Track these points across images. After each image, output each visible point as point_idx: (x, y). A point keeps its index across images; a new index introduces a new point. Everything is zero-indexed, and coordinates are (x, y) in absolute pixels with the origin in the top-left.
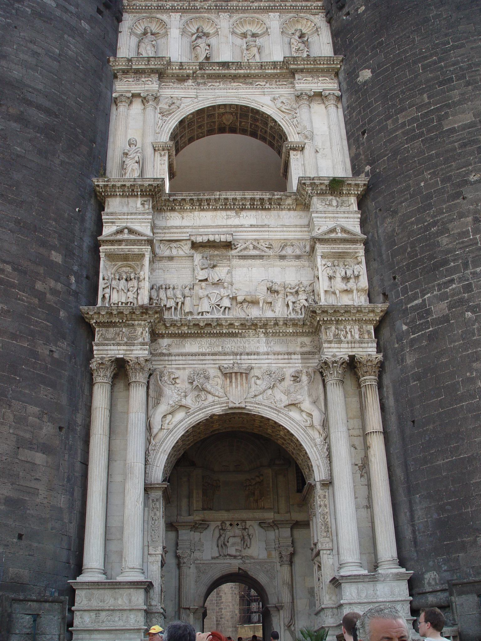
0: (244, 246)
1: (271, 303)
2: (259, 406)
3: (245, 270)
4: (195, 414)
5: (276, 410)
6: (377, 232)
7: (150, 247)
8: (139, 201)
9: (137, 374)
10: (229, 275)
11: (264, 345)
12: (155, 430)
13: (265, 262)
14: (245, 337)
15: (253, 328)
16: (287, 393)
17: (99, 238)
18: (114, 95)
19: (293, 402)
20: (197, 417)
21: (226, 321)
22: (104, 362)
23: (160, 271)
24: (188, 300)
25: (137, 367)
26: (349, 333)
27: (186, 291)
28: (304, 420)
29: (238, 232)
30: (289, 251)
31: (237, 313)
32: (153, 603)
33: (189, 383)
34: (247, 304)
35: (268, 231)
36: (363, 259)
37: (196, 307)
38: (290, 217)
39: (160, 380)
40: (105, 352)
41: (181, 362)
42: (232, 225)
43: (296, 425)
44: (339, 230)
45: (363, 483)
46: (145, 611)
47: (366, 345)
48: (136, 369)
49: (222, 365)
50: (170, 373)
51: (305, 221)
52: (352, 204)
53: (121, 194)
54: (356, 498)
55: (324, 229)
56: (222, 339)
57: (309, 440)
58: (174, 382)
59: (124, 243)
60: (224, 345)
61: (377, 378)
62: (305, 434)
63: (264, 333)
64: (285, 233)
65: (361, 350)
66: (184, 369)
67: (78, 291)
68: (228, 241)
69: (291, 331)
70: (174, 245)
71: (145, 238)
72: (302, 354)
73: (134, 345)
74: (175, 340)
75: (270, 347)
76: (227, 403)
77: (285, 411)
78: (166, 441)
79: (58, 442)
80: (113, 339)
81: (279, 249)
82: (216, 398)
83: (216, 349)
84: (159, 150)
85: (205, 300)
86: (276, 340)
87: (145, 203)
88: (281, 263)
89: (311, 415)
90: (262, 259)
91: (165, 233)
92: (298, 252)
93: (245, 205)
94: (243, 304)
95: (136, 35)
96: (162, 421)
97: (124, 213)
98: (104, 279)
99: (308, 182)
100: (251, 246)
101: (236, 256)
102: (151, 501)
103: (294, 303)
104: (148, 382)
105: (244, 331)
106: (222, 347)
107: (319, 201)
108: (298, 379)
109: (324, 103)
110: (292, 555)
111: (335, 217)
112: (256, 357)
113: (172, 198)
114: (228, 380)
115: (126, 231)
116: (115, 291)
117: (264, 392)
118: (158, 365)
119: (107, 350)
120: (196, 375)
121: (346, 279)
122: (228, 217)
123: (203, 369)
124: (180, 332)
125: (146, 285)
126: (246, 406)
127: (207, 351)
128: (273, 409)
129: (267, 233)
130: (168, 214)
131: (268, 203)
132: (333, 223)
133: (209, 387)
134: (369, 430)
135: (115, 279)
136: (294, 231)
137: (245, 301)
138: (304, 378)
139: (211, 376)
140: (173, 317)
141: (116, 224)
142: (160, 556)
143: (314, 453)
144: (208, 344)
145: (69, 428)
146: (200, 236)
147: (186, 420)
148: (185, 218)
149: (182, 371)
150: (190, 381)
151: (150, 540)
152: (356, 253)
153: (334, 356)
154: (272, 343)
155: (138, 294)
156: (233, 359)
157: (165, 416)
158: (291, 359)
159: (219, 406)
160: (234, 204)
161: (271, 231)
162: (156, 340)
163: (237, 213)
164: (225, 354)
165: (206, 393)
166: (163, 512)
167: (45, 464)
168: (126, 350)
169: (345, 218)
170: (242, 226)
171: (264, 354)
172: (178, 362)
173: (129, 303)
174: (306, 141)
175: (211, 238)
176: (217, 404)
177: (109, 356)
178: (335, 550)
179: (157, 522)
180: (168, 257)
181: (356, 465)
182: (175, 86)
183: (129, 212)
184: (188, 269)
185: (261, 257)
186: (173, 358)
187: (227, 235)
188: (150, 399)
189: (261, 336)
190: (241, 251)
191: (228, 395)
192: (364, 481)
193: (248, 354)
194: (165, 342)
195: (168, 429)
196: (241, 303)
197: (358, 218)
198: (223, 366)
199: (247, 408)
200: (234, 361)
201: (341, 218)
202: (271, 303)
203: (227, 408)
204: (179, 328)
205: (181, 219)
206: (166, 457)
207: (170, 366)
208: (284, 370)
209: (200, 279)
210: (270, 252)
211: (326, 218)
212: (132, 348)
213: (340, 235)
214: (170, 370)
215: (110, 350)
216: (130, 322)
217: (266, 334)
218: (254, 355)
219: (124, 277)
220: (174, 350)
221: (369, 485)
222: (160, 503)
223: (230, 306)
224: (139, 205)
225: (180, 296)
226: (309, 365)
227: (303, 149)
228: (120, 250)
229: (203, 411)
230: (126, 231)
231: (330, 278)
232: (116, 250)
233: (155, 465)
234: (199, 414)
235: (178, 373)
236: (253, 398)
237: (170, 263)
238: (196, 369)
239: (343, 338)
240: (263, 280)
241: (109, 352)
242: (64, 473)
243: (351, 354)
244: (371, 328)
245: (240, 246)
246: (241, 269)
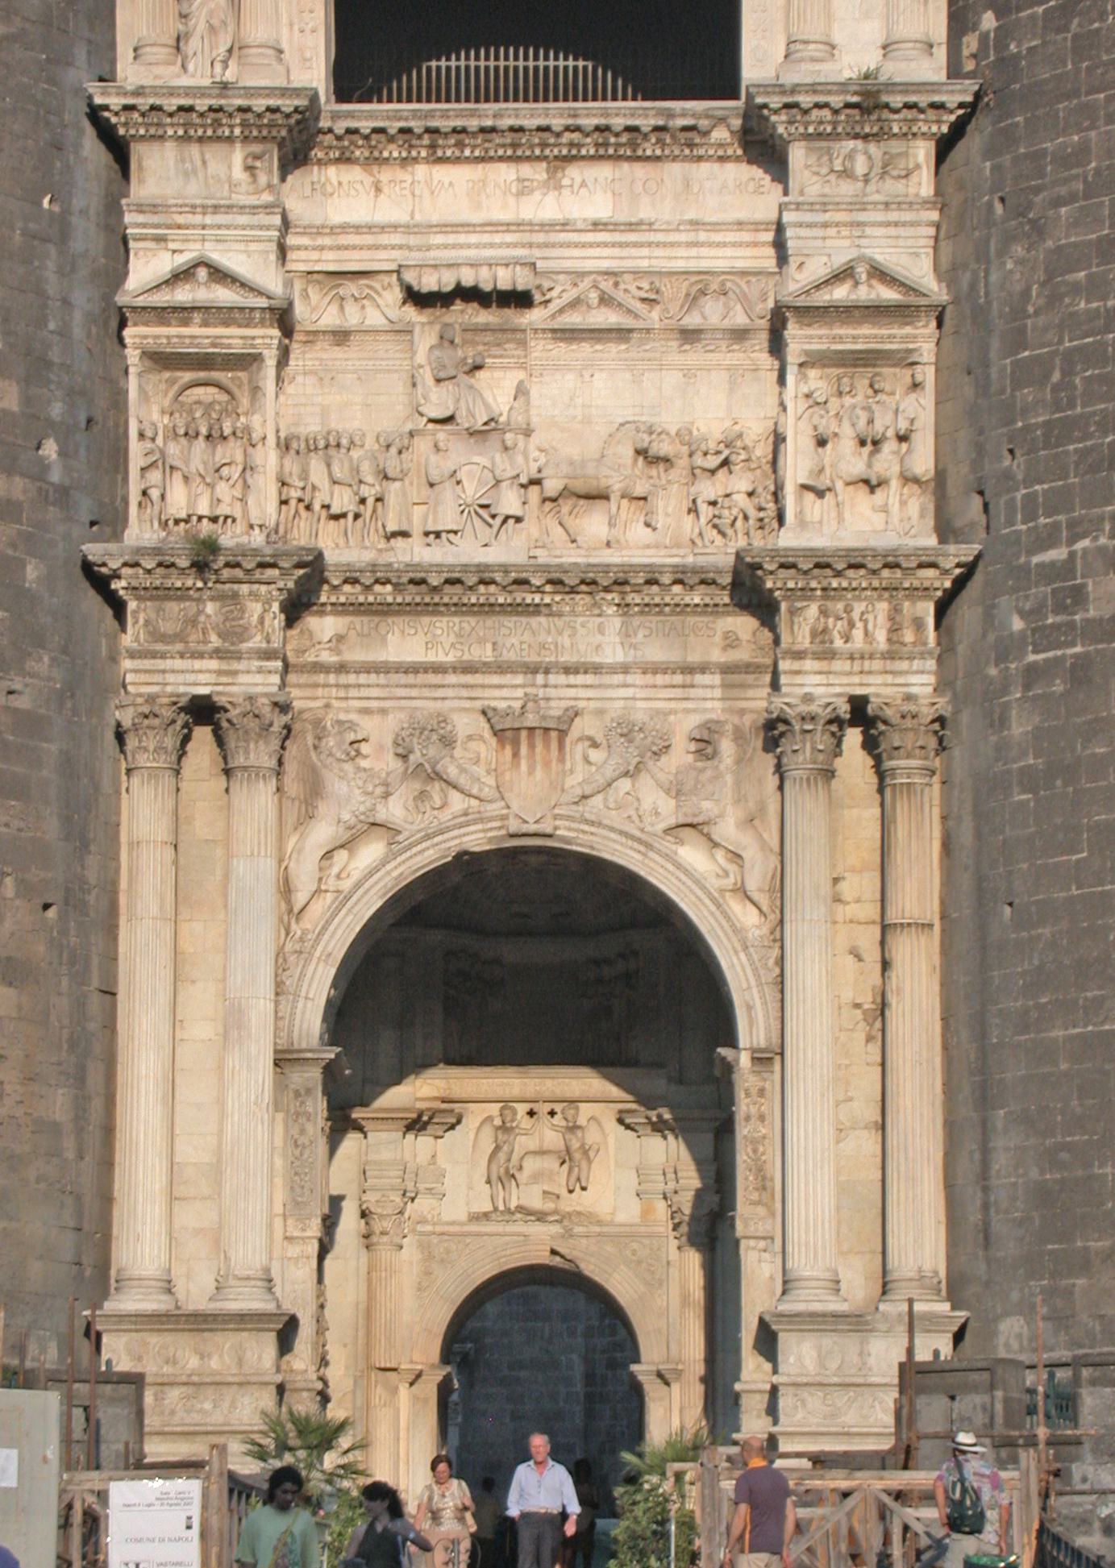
0: (572, 294)
2: (593, 829)
3: (570, 380)
4: (414, 850)
5: (639, 841)
6: (986, 277)
7: (276, 332)
8: (238, 155)
9: (252, 746)
10: (521, 400)
11: (618, 639)
12: (300, 899)
14: (560, 615)
15: (584, 588)
16: (677, 791)
19: (689, 820)
20: (419, 858)
22: (156, 709)
23: (311, 380)
25: (253, 724)
26: (859, 625)
27: (388, 463)
28: (720, 873)
29: (553, 245)
30: (711, 313)
33: (397, 755)
34: (571, 502)
35: (650, 244)
36: (930, 371)
38: (724, 186)
39: (315, 747)
40: (158, 678)
41: (374, 692)
42: (536, 221)
43: (694, 887)
44: (861, 271)
47: (904, 665)
49: (493, 704)
50: (343, 726)
52: (918, 167)
53: (181, 132)
55: (817, 268)
56: (491, 621)
57: (729, 931)
58: (353, 753)
59: (197, 317)
60: (500, 640)
62: (718, 913)
63: (618, 605)
64: (704, 251)
65: (889, 679)
66: (383, 712)
67: (67, 482)
68: (520, 288)
69: (697, 600)
70: (350, 288)
71: (263, 302)
72: (727, 669)
73: (240, 658)
75: (634, 646)
76: (504, 818)
77: (667, 845)
78: (332, 928)
79: (42, 949)
80: (180, 637)
81: (682, 306)
82: (474, 803)
85: (448, 492)
86: (653, 626)
87: (258, 164)
88: (682, 357)
89: (739, 856)
90: (627, 340)
91: (322, 248)
92: (740, 319)
93: (579, 146)
94: (560, 501)
96: (321, 869)
97: (194, 206)
98: (142, 436)
99: (775, 102)
100: (594, 296)
101: (544, 330)
102: (291, 1095)
103: (713, 503)
105: (558, 598)
106: (494, 644)
107: (812, 160)
108: (709, 750)
111: (859, 224)
112: (589, 679)
114: (508, 751)
115: (202, 273)
116: (178, 476)
117: (609, 785)
119: (164, 672)
120: (417, 732)
122: (524, 189)
123: (439, 715)
124: (371, 599)
126: (556, 828)
127: (450, 658)
129: (645, 251)
130: (332, 171)
131: (653, 140)
132: (847, 243)
133: (452, 772)
136: (734, 245)
137: (567, 493)
141: (172, 246)
143: (738, 968)
144: (452, 636)
145: (67, 903)
146: (431, 270)
147: (389, 867)
148: (386, 189)
149: (377, 719)
150: (400, 751)
152: (910, 351)
153: (808, 698)
154: (640, 635)
155: (246, 486)
156: (523, 686)
157: (328, 855)
158: (693, 686)
159: (479, 827)
160: (544, 145)
161: (658, 245)
162: (298, 618)
163: (552, 172)
164: (502, 668)
165: (444, 785)
167: (14, 1015)
168: (220, 673)
169: (888, 224)
170: (565, 226)
171: (613, 669)
172: (364, 692)
173: (221, 519)
175: (468, 278)
176: (475, 822)
177: (169, 689)
179: (307, 1153)
180: (334, 333)
181: (857, 1006)
183: (210, 202)
184: (396, 376)
185: (621, 334)
186: (352, 678)
187: (518, 268)
189: (610, 612)
190: (561, 311)
191: (506, 795)
193: (568, 670)
195: (338, 891)
196: (554, 500)
197: (930, 224)
198: (495, 710)
199: (558, 832)
200: (529, 690)
201: (874, 224)
202: (645, 499)
203: (503, 832)
204: (368, 588)
205: (373, 193)
206: (333, 971)
207: (343, 704)
208: (672, 718)
209: (434, 415)
211: (825, 225)
214: (342, 717)
215: (173, 671)
216: (228, 586)
217: (624, 607)
218: (586, 672)
219: (204, 431)
220: (356, 655)
223: (519, 513)
224: (238, 173)
225: (370, 479)
228: (187, 341)
229: (436, 840)
230: (202, 273)
232: (175, 340)
233: (303, 994)
234: (424, 850)
235: (368, 726)
236: (576, 803)
237: (338, 352)
238: (418, 713)
239: (838, 643)
240: (622, 425)
241: (170, 678)
242: (62, 1028)
243: (859, 691)
244: (927, 610)
245: (562, 293)
246: (558, 376)
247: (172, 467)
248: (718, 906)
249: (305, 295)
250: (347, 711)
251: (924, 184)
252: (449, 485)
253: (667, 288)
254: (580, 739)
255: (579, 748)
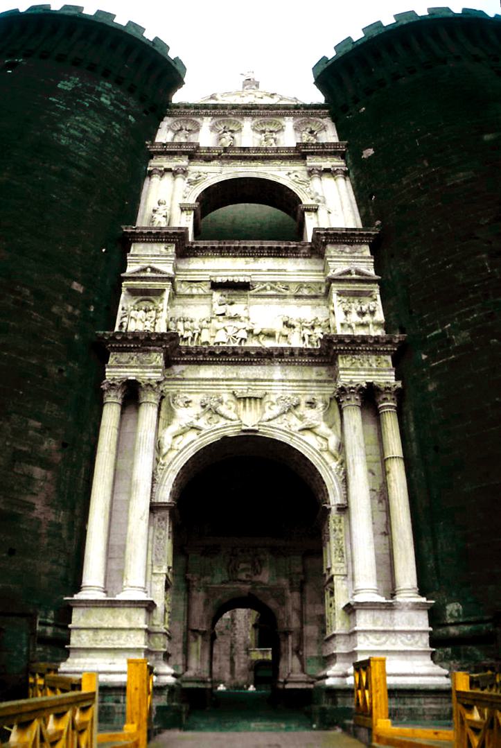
0: (262, 287)
1: (287, 336)
7: (170, 283)
12: (164, 450)
13: (282, 301)
16: (301, 418)
17: (123, 275)
18: (148, 169)
19: (308, 427)
21: (242, 350)
24: (204, 332)
29: (255, 275)
31: (253, 343)
32: (156, 622)
37: (212, 339)
39: (173, 403)
45: (381, 509)
46: (147, 631)
48: (148, 390)
51: (321, 268)
54: (373, 523)
55: (339, 271)
61: (395, 405)
70: (195, 285)
74: (190, 367)
75: (286, 375)
82: (229, 422)
83: (230, 376)
84: (186, 210)
95: (173, 131)
98: (123, 309)
100: (268, 288)
103: (310, 336)
104: (160, 404)
108: (313, 406)
109: (334, 177)
110: (303, 583)
113: (194, 246)
114: (242, 404)
115: (149, 270)
116: (133, 320)
118: (170, 389)
121: (362, 314)
125: (164, 316)
128: (288, 433)
134: (388, 455)
135: (135, 310)
137: (261, 333)
138: (320, 405)
139: (225, 400)
140: (190, 345)
142: (165, 576)
149: (196, 395)
150: (203, 404)
151: (154, 559)
152: (371, 291)
155: (155, 323)
156: (247, 385)
157: (175, 437)
164: (239, 380)
166: (169, 532)
170: (259, 270)
174: (319, 204)
175: (231, 279)
178: (350, 576)
179: (162, 542)
181: (374, 490)
182: (202, 164)
186: (187, 383)
188: (161, 420)
190: (259, 291)
191: (241, 418)
192: (382, 507)
194: (177, 369)
202: (287, 336)
206: (175, 476)
207: (183, 390)
210: (288, 293)
212: (145, 370)
213: (354, 276)
219: (143, 308)
221: (388, 511)
222: (166, 522)
223: (246, 338)
226: (326, 392)
227: (316, 211)
230: (149, 270)
231: (346, 313)
241: (122, 374)
243: (368, 381)
245: (258, 287)
247: (132, 318)
248: (320, 455)
249: (181, 287)
250: (185, 393)
251: (368, 253)
252: (223, 330)
253: (291, 286)
254: (268, 402)
255: (268, 404)
